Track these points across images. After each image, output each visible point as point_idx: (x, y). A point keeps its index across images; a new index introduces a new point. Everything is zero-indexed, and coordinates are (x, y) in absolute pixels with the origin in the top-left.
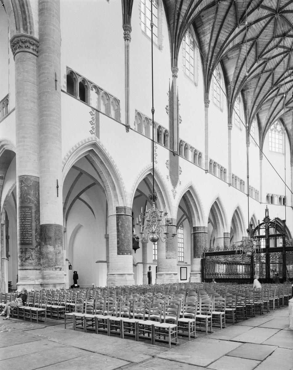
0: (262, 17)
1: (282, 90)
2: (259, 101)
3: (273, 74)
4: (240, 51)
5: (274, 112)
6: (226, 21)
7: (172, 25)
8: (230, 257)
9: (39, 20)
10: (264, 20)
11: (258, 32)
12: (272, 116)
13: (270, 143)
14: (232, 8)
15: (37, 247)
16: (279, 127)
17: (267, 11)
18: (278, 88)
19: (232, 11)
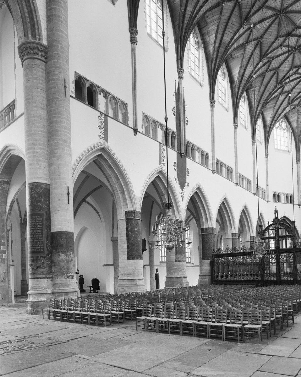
0: (266, 17)
1: (287, 88)
2: (264, 100)
3: (278, 73)
4: (245, 50)
5: (279, 110)
6: (230, 22)
7: (177, 27)
8: (239, 258)
9: (47, 26)
10: (268, 20)
11: (262, 32)
12: (277, 114)
13: (275, 141)
14: (236, 9)
15: (48, 255)
16: (284, 125)
17: (271, 11)
18: (283, 87)
19: (236, 12)
